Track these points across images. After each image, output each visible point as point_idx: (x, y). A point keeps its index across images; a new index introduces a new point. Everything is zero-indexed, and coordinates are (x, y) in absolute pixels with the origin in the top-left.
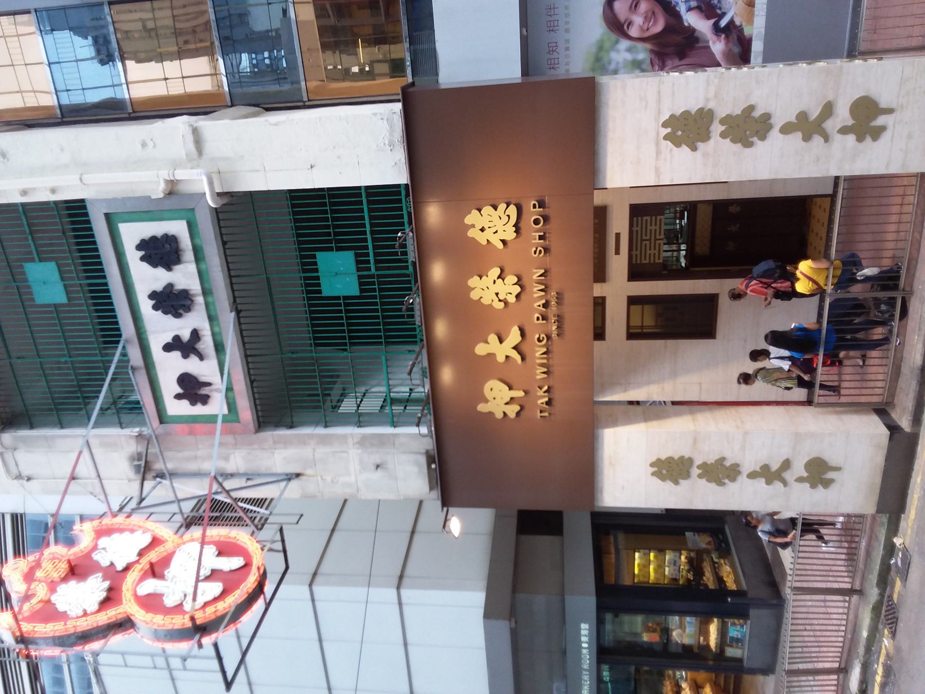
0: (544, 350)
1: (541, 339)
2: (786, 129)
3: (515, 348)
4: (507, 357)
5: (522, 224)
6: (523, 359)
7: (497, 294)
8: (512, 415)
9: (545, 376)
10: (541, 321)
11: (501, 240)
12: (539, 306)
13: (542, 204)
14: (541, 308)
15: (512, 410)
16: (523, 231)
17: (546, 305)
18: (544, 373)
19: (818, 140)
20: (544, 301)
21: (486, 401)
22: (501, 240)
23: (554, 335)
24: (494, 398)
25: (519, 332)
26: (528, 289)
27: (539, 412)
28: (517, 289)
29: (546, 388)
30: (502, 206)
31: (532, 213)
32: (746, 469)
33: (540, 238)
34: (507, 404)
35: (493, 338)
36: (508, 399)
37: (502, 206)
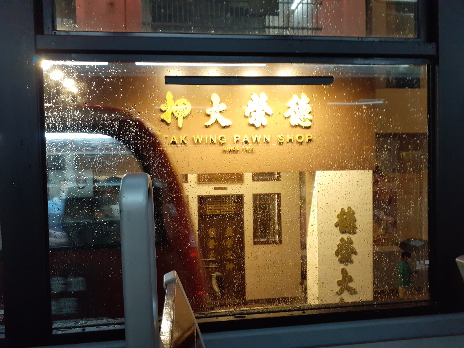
0: (215, 141)
1: (223, 139)
2: (344, 272)
3: (216, 121)
4: (209, 116)
5: (298, 129)
6: (207, 127)
7: (255, 111)
8: (163, 116)
9: (196, 141)
10: (235, 139)
11: (290, 116)
12: (174, 139)
13: (310, 140)
14: (172, 140)
15: (167, 117)
16: (294, 129)
17: (246, 142)
18: (198, 140)
19: (338, 288)
20: (177, 142)
21: (175, 99)
22: (290, 116)
23: (224, 148)
24: (177, 105)
25: (227, 125)
26: (256, 131)
27: (167, 136)
28: (258, 125)
29: (185, 142)
30: (310, 117)
31: (306, 136)
32: (350, 268)
33: (290, 140)
34: (172, 113)
35: (223, 107)
36: (176, 115)
37: (310, 117)
